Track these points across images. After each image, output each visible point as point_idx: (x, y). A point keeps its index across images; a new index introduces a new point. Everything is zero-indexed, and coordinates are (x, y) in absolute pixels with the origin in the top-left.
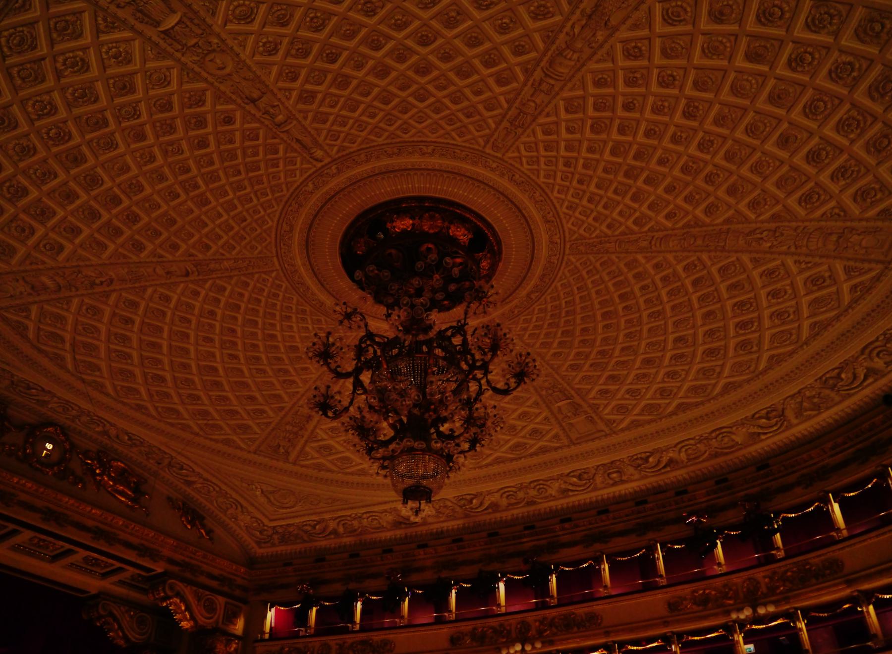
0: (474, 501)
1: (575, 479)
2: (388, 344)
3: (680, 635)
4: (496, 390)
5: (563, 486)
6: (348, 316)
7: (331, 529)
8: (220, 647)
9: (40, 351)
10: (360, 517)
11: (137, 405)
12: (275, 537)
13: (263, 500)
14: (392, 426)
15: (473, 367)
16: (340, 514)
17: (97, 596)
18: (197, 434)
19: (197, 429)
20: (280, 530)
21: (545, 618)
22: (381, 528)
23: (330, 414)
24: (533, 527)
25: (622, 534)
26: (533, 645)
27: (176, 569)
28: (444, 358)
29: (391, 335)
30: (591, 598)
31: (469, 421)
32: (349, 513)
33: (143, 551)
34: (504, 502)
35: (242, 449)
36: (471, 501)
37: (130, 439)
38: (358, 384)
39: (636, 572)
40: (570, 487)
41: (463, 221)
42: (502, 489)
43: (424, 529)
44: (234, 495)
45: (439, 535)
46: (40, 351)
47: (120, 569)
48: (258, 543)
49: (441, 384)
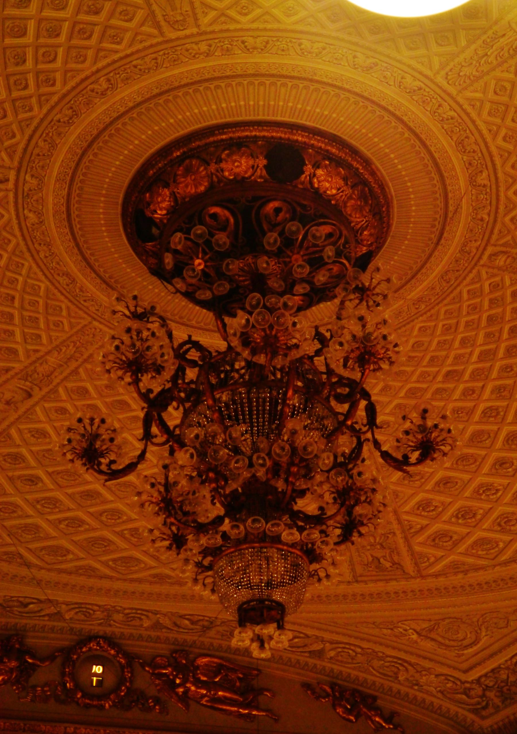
11: (155, 576)
12: (491, 694)
13: (429, 645)
41: (237, 145)
44: (389, 652)
48: (475, 712)
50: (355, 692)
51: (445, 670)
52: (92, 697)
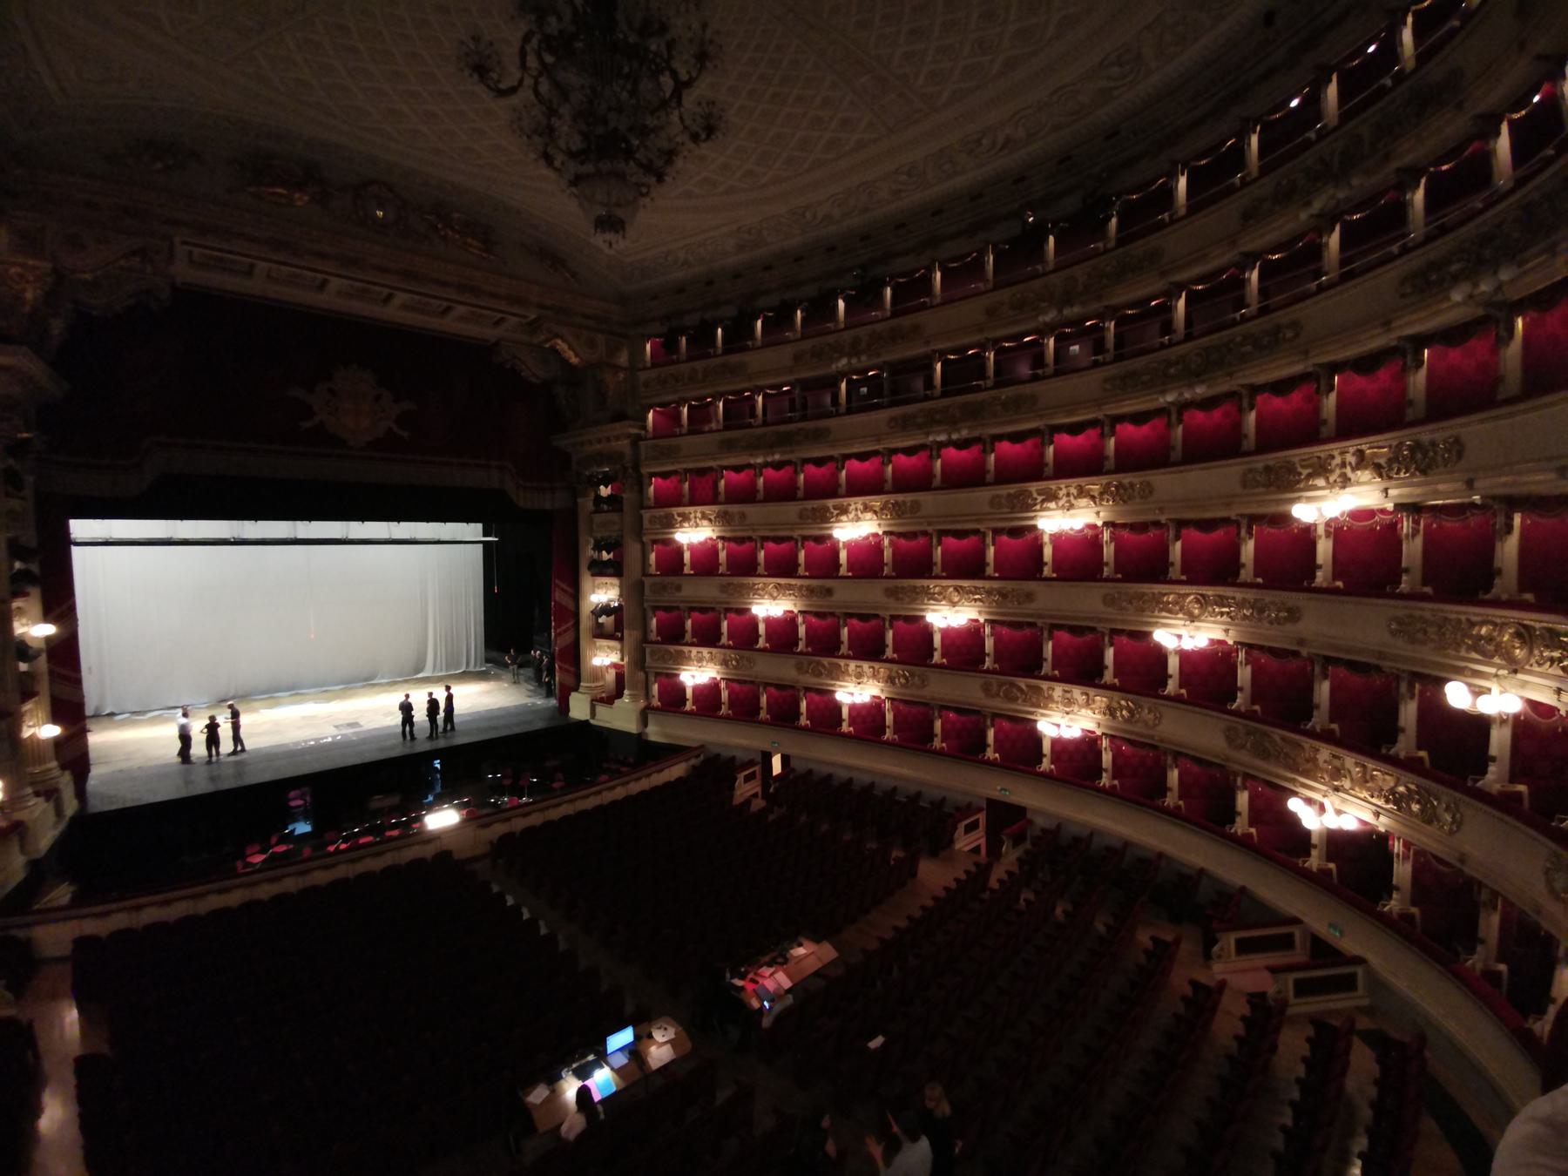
3: (996, 341)
36: (803, 215)
47: (501, 320)
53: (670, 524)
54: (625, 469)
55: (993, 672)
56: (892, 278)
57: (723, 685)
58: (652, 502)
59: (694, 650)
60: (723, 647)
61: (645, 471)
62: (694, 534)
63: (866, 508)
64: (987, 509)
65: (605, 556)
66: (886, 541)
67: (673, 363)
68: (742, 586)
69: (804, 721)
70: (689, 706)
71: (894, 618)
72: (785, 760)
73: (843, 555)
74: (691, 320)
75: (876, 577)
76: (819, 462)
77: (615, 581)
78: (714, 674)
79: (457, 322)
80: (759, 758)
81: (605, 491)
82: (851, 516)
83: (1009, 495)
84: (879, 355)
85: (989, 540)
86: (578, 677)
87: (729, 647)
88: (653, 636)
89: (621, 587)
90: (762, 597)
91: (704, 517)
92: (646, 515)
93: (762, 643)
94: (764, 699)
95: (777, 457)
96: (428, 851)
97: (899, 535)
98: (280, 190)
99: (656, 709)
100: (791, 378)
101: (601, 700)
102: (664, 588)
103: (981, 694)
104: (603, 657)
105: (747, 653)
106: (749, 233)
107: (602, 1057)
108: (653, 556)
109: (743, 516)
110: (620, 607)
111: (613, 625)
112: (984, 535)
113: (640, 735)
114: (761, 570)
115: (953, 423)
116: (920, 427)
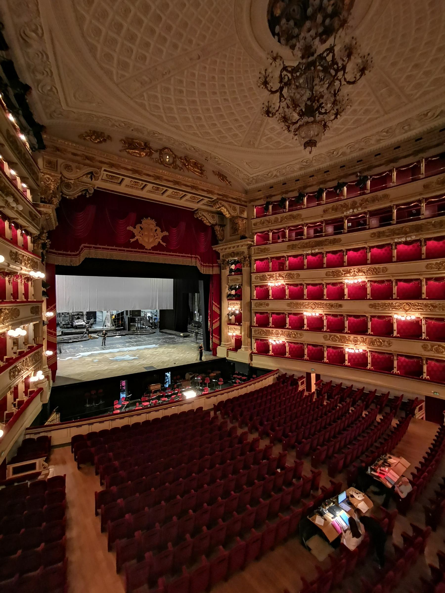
0: (335, 153)
1: (385, 133)
2: (294, 70)
3: (426, 199)
4: (349, 83)
5: (378, 138)
6: (275, 59)
7: (274, 174)
8: (240, 222)
9: (153, 115)
10: (286, 168)
11: (194, 133)
13: (247, 166)
14: (299, 114)
15: (337, 71)
16: (278, 167)
17: (197, 210)
18: (218, 142)
19: (218, 140)
20: (255, 178)
21: (363, 199)
22: (293, 172)
23: (271, 115)
24: (361, 160)
25: (405, 157)
26: (357, 209)
27: (221, 197)
28: (322, 71)
29: (295, 64)
30: (386, 188)
31: (334, 103)
32: (281, 167)
33: (209, 192)
34: (348, 151)
35: (236, 145)
37: (194, 149)
38: (281, 96)
39: (410, 173)
40: (382, 138)
42: (347, 145)
43: (312, 169)
45: (318, 171)
46: (153, 115)
48: (248, 184)
49: (321, 88)
50: (223, 175)
51: (246, 173)
52: (167, 164)
53: (264, 278)
54: (245, 258)
55: (427, 340)
56: (371, 177)
57: (287, 345)
58: (255, 271)
59: (275, 330)
60: (288, 329)
61: (253, 258)
62: (276, 282)
63: (359, 271)
64: (424, 269)
65: (233, 292)
66: (368, 285)
67: (265, 216)
68: (297, 304)
69: (326, 360)
70: (271, 353)
71: (372, 317)
72: (318, 377)
73: (346, 291)
74: (278, 198)
75: (363, 299)
76: (334, 252)
77: (239, 302)
78: (284, 340)
79: (185, 203)
80: (305, 375)
81: (233, 267)
82: (352, 274)
83: (437, 263)
84: (366, 208)
85: (424, 283)
86: (220, 340)
87: (290, 329)
88: (255, 324)
89: (241, 304)
90: (307, 308)
91: (280, 276)
92: (253, 276)
93: (305, 327)
94: (306, 351)
95: (317, 251)
96: (185, 408)
97: (375, 282)
98: (136, 151)
99: (255, 353)
100: (322, 219)
101: (230, 350)
102: (261, 304)
103: (422, 350)
104: (232, 333)
105: (299, 332)
106: (306, 162)
107: (337, 506)
108: (255, 292)
109: (298, 275)
110: (240, 313)
111: (238, 320)
112: (421, 281)
113: (249, 364)
114: (305, 297)
115: (406, 234)
116: (387, 236)
